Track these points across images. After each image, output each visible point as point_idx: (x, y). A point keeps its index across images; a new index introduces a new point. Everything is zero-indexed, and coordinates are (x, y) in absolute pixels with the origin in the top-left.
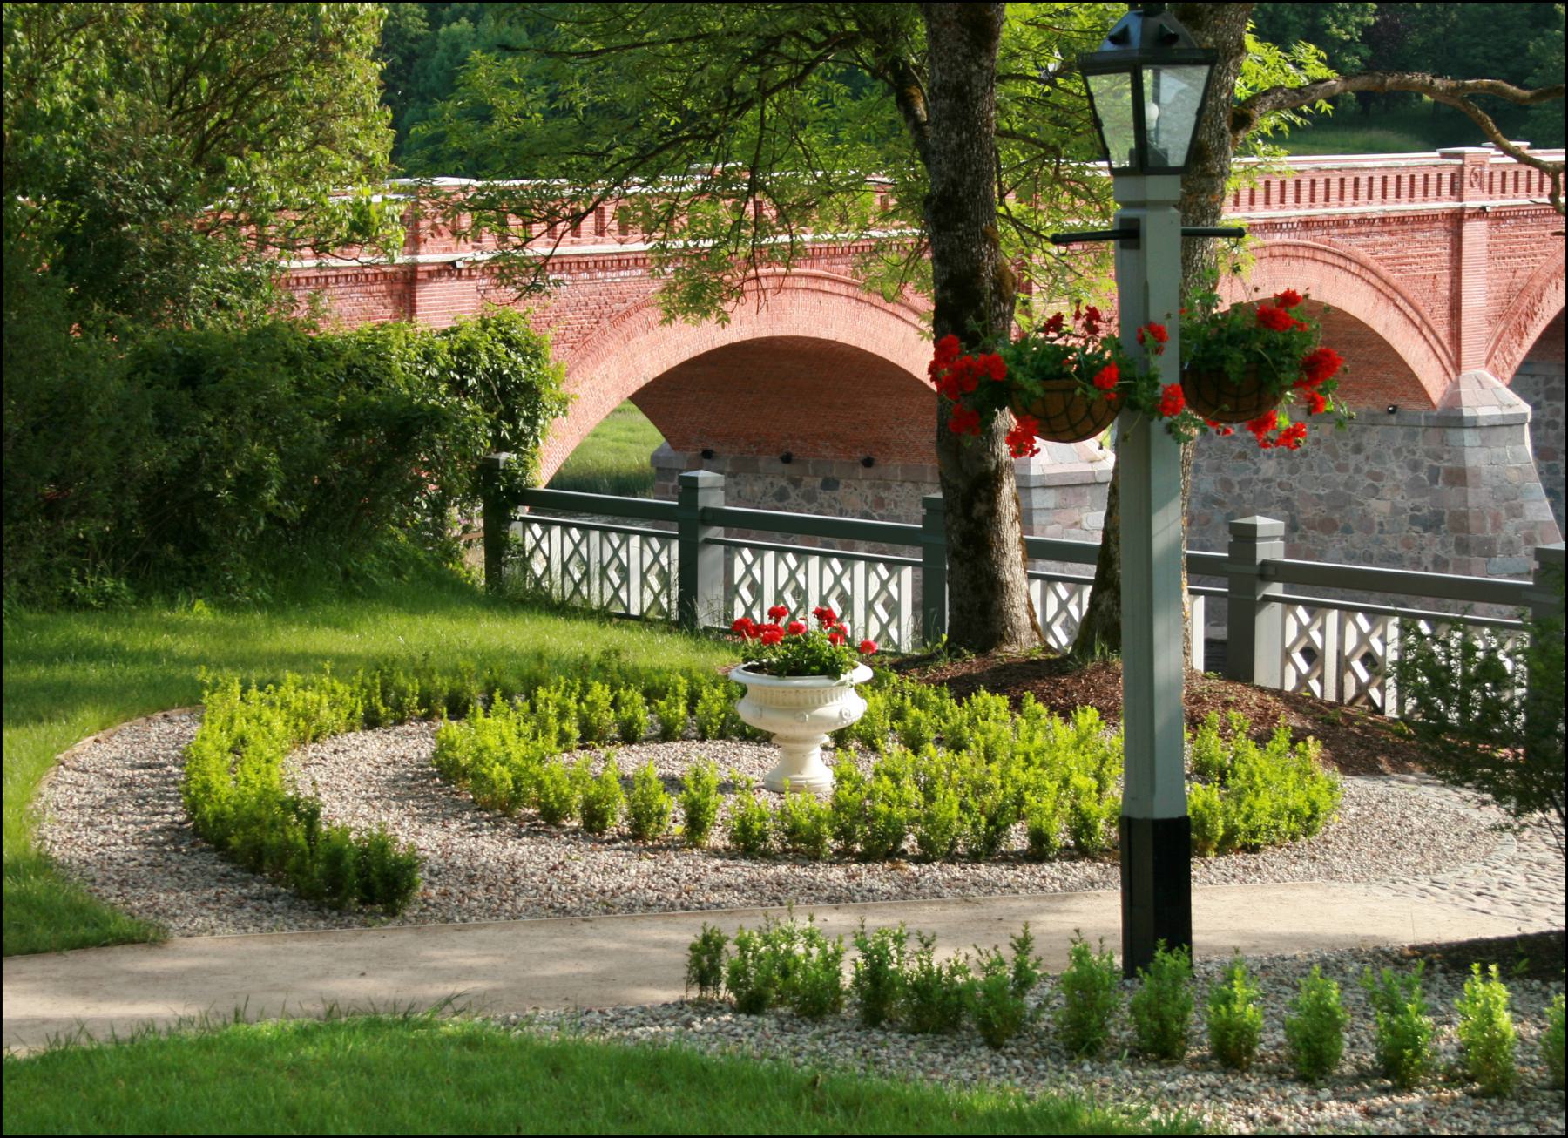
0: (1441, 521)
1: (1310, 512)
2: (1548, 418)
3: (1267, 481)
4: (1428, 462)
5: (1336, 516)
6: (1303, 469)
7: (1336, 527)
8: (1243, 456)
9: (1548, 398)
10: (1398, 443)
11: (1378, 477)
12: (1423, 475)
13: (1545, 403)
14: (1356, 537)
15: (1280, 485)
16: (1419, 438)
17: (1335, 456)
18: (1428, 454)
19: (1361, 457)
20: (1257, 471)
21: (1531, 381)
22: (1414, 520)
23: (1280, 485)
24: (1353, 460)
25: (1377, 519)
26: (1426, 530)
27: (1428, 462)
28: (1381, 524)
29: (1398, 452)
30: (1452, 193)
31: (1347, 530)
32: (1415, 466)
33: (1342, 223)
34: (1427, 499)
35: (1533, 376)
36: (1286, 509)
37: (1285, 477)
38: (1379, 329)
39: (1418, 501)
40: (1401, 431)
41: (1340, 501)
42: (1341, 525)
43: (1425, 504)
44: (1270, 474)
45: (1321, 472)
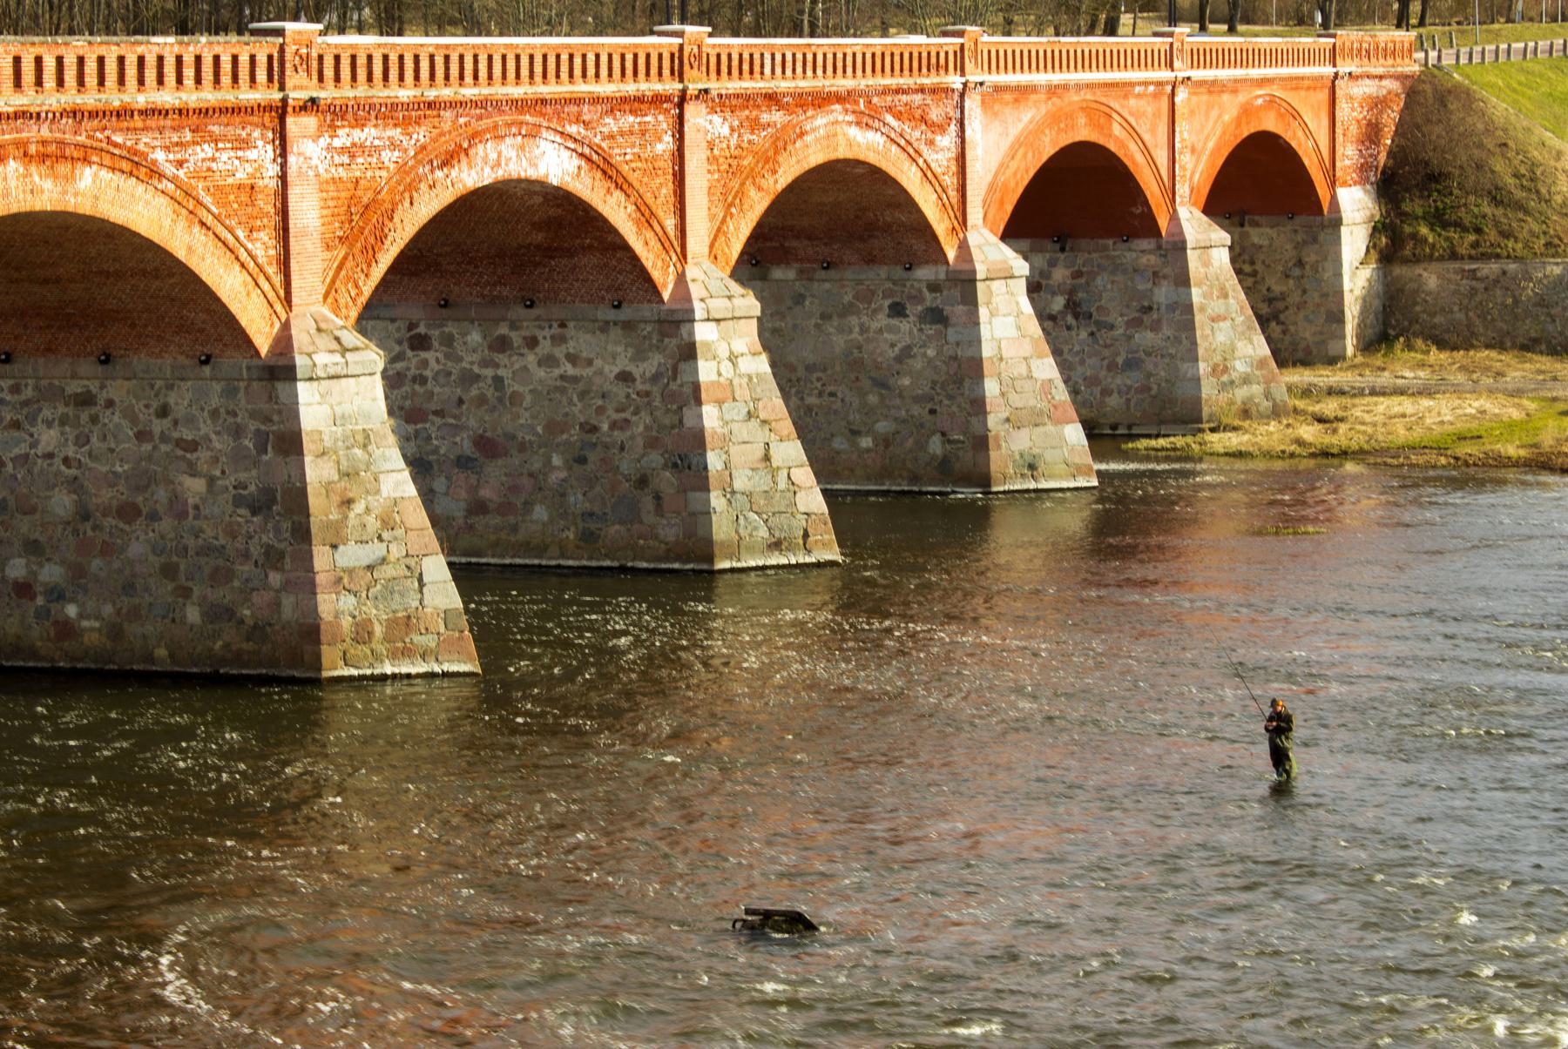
0: (273, 501)
1: (106, 496)
2: (413, 372)
3: (50, 456)
4: (253, 426)
5: (140, 499)
6: (94, 440)
7: (139, 513)
8: (16, 425)
9: (413, 348)
10: (215, 401)
11: (193, 446)
12: (248, 443)
13: (410, 353)
14: (166, 525)
15: (66, 461)
16: (241, 394)
17: (134, 420)
18: (253, 415)
19: (167, 422)
20: (34, 445)
21: (391, 327)
22: (238, 501)
23: (66, 461)
24: (158, 426)
25: (191, 501)
26: (254, 514)
27: (253, 426)
28: (196, 507)
29: (215, 414)
30: (270, 79)
31: (154, 517)
32: (238, 432)
33: (123, 113)
34: (254, 473)
35: (393, 320)
36: (75, 492)
37: (71, 451)
38: (181, 255)
39: (243, 476)
40: (217, 387)
41: (143, 481)
42: (145, 511)
43: (252, 479)
44: (50, 449)
45: (118, 442)
